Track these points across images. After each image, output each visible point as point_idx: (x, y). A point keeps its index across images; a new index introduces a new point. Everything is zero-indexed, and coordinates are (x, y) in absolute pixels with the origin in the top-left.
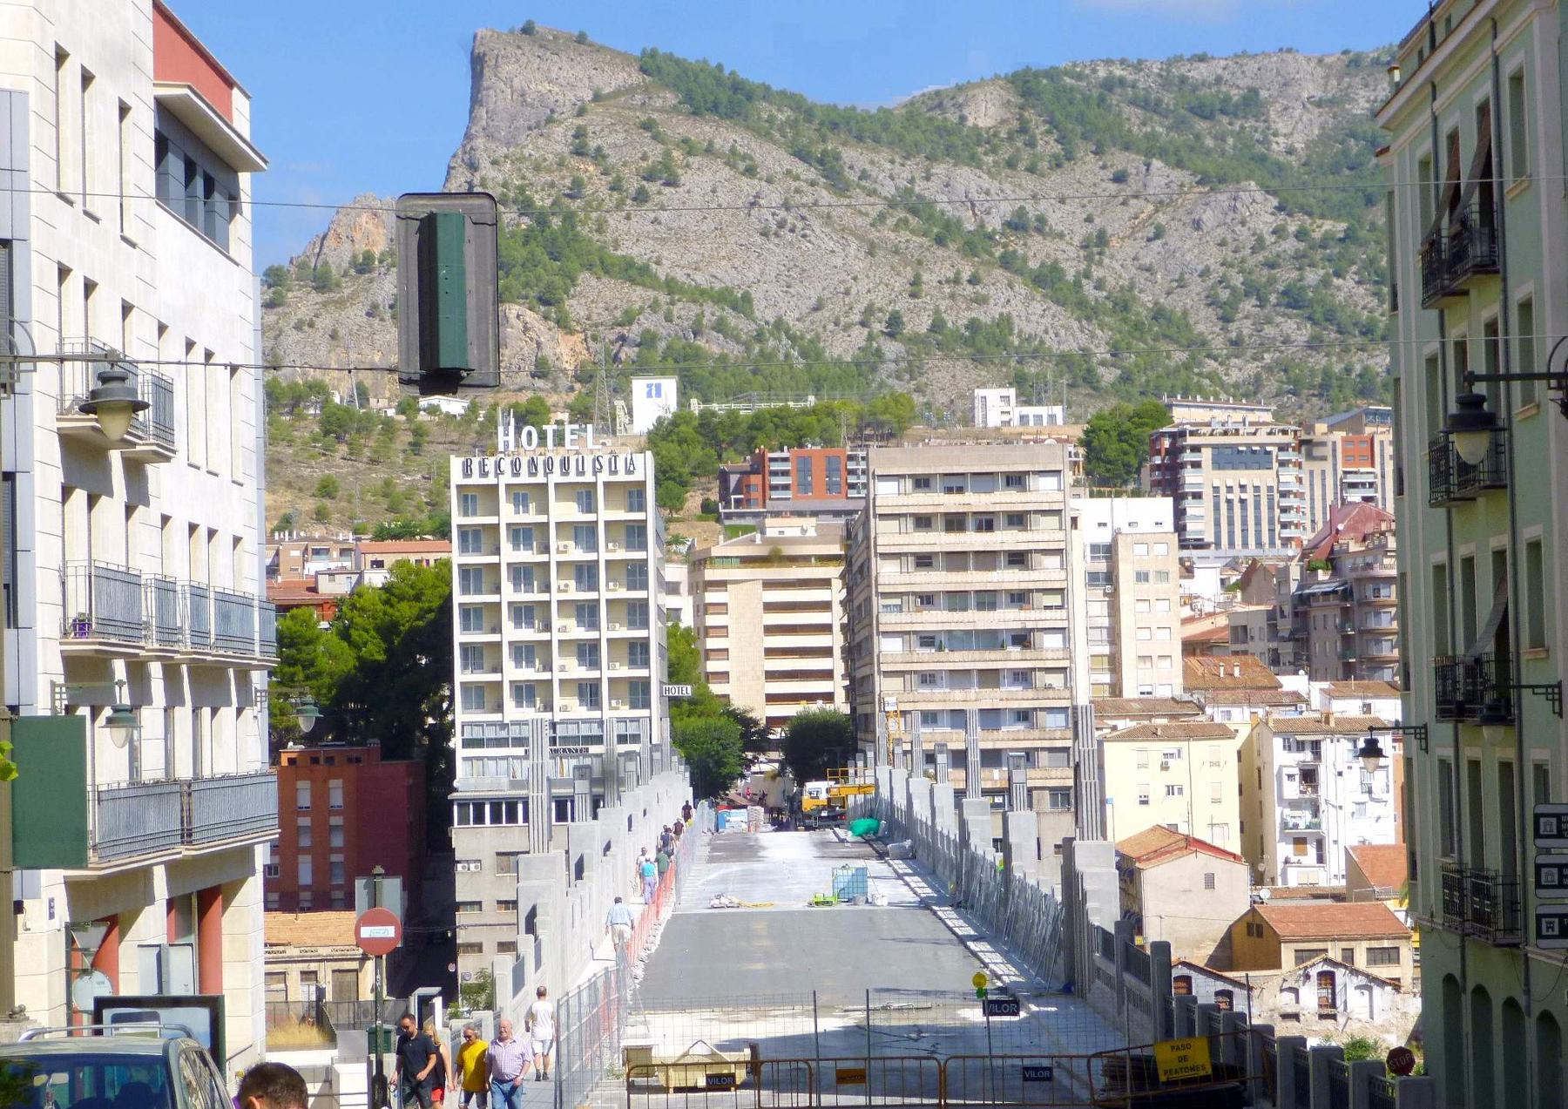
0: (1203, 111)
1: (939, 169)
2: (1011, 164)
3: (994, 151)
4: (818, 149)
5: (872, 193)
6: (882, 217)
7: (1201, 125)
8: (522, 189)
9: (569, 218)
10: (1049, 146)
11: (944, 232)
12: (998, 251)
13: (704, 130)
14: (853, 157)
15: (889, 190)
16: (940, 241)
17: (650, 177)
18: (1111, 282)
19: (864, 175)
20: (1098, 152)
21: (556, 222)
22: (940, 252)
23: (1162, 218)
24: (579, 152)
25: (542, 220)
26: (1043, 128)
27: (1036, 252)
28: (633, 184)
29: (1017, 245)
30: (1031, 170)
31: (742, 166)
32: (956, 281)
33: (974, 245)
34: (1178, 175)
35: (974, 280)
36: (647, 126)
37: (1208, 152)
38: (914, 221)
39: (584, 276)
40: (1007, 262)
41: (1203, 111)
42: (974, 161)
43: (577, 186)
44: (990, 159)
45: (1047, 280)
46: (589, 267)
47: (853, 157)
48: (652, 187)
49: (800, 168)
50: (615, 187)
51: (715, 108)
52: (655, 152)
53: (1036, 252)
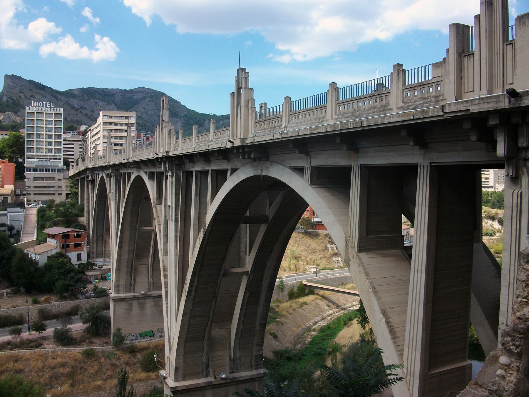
0: (107, 95)
1: (71, 99)
2: (81, 100)
3: (79, 98)
4: (54, 95)
6: (64, 105)
8: (11, 97)
9: (19, 101)
10: (87, 98)
11: (73, 108)
12: (79, 111)
13: (39, 91)
14: (59, 96)
15: (64, 101)
17: (31, 96)
18: (94, 116)
19: (61, 99)
20: (93, 99)
21: (17, 102)
23: (101, 108)
24: (21, 92)
25: (15, 102)
27: (85, 112)
28: (28, 97)
29: (82, 110)
30: (84, 101)
32: (74, 114)
33: (77, 110)
34: (103, 103)
35: (77, 114)
37: (107, 101)
38: (68, 106)
39: (21, 109)
40: (81, 112)
41: (107, 95)
42: (76, 99)
43: (20, 97)
44: (78, 99)
45: (86, 115)
46: (22, 108)
47: (59, 96)
49: (52, 97)
50: (26, 97)
52: (31, 93)
53: (85, 112)
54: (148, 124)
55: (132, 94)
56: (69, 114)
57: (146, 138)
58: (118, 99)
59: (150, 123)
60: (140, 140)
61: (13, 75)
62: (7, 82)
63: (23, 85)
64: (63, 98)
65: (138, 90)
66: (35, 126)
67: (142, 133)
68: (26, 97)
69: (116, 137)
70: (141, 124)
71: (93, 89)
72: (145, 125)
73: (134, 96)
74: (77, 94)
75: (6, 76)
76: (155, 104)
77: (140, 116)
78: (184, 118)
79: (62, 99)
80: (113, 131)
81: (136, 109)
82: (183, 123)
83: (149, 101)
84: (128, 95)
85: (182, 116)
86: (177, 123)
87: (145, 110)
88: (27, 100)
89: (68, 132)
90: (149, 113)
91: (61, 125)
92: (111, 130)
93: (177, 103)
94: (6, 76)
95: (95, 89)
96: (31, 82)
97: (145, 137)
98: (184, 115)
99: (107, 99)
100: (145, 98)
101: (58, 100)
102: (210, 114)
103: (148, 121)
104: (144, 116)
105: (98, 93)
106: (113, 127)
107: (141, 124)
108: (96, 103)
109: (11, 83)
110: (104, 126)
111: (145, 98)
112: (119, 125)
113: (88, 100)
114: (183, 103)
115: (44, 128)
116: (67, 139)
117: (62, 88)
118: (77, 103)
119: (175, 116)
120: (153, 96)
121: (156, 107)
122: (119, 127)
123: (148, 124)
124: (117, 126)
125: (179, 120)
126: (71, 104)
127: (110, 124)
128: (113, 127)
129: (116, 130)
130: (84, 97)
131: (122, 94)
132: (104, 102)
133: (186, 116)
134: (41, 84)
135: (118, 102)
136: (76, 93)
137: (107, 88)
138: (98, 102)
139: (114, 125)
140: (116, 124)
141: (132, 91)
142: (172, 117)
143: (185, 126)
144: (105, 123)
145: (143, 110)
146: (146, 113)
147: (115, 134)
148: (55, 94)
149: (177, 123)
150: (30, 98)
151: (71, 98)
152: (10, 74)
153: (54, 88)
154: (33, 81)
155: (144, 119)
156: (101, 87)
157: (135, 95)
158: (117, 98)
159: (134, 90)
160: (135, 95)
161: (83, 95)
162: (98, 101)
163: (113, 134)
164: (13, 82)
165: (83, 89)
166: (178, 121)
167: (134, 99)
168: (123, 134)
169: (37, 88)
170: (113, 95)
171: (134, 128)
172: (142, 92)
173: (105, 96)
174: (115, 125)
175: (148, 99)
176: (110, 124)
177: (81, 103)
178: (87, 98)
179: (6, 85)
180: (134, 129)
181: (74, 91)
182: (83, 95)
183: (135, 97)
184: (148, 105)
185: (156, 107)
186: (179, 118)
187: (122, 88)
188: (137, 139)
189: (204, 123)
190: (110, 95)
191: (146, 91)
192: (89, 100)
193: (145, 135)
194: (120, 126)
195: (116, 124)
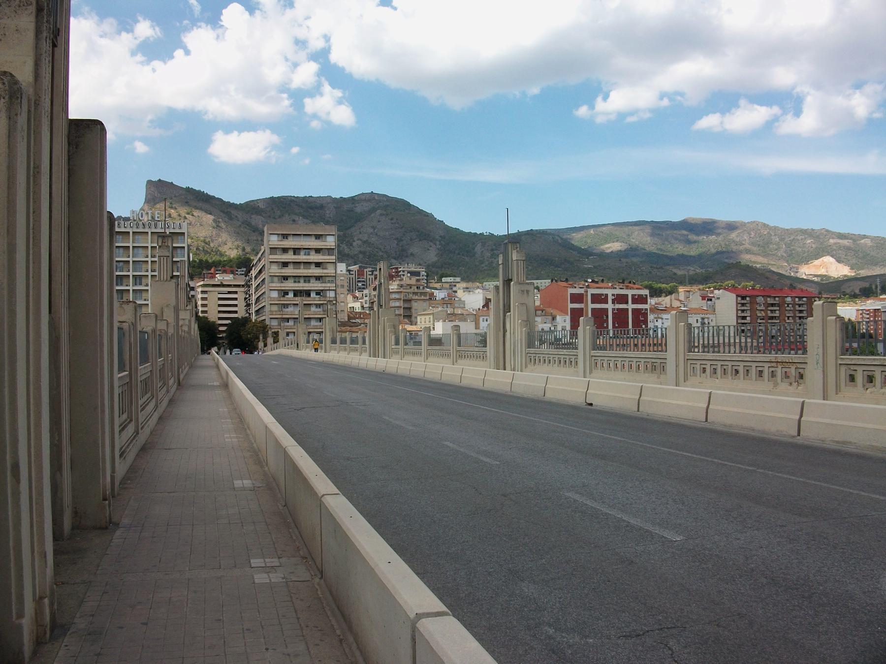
0: (311, 208)
2: (270, 217)
3: (266, 213)
5: (238, 221)
6: (240, 226)
7: (311, 211)
10: (278, 213)
14: (233, 212)
16: (254, 231)
17: (188, 214)
19: (236, 217)
22: (254, 234)
26: (277, 209)
30: (274, 218)
31: (209, 212)
32: (257, 240)
36: (187, 202)
38: (247, 227)
42: (261, 215)
47: (233, 212)
48: (187, 216)
49: (222, 214)
51: (203, 200)
54: (381, 254)
55: (353, 203)
56: (248, 240)
57: (373, 277)
58: (329, 213)
59: (383, 252)
60: (363, 281)
61: (160, 180)
62: (151, 192)
63: (175, 196)
64: (240, 215)
65: (363, 197)
66: (130, 259)
67: (366, 268)
68: (179, 215)
69: (297, 278)
70: (368, 254)
71: (289, 198)
72: (375, 255)
73: (355, 207)
74: (262, 207)
75: (150, 183)
76: (392, 219)
77: (367, 240)
78: (440, 241)
79: (238, 216)
80: (291, 266)
81: (360, 229)
82: (438, 249)
83: (381, 215)
84: (346, 207)
85: (437, 237)
86: (428, 250)
87: (374, 230)
88: (180, 219)
89: (239, 270)
90: (381, 235)
91: (184, 257)
92: (285, 264)
93: (428, 216)
94: (150, 183)
95: (293, 198)
96: (189, 190)
97: (372, 274)
98: (441, 237)
99: (312, 215)
100: (373, 210)
101: (231, 219)
102: (485, 232)
103: (380, 249)
104: (373, 239)
105: (297, 205)
106: (289, 257)
107: (368, 254)
108: (294, 221)
109: (156, 193)
110: (271, 257)
111: (373, 210)
112: (302, 252)
113: (280, 217)
114: (438, 216)
115: (150, 263)
116: (225, 283)
117: (238, 198)
118: (262, 221)
119: (425, 239)
120: (388, 206)
121: (392, 223)
122: (302, 257)
123: (381, 254)
124: (299, 254)
125: (432, 244)
126: (253, 223)
127: (285, 250)
128: (289, 257)
129: (297, 264)
130: (274, 212)
131: (335, 205)
132: (307, 219)
133: (443, 237)
134: (205, 192)
135: (330, 218)
136: (261, 205)
137: (311, 196)
138: (298, 219)
139: (291, 252)
140: (297, 251)
141: (352, 199)
142: (420, 240)
143: (442, 255)
144: (273, 250)
145: (371, 230)
146: (377, 234)
147: (306, 271)
148: (227, 208)
149: (428, 250)
150: (187, 216)
151: (252, 214)
152: (155, 179)
153: (226, 199)
154: (192, 188)
155: (373, 244)
156: (301, 194)
157: (357, 205)
158: (328, 212)
159: (356, 198)
160: (357, 205)
161: (272, 209)
162: (296, 218)
163: (289, 271)
164: (160, 193)
165: (272, 198)
166: (431, 246)
167: (357, 213)
168: (310, 271)
169: (198, 201)
170: (322, 207)
171: (334, 257)
172: (369, 200)
173: (309, 210)
174: (294, 254)
175: (379, 212)
176: (285, 250)
177: (268, 221)
178: (278, 213)
179: (149, 196)
180: (334, 261)
181: (258, 203)
182: (272, 209)
183: (358, 210)
184: (379, 221)
185: (392, 223)
186: (431, 241)
187: (336, 195)
188: (358, 278)
189: (474, 249)
190: (317, 208)
191: (376, 198)
192: (283, 216)
193: (372, 271)
194: (305, 254)
195: (296, 251)
